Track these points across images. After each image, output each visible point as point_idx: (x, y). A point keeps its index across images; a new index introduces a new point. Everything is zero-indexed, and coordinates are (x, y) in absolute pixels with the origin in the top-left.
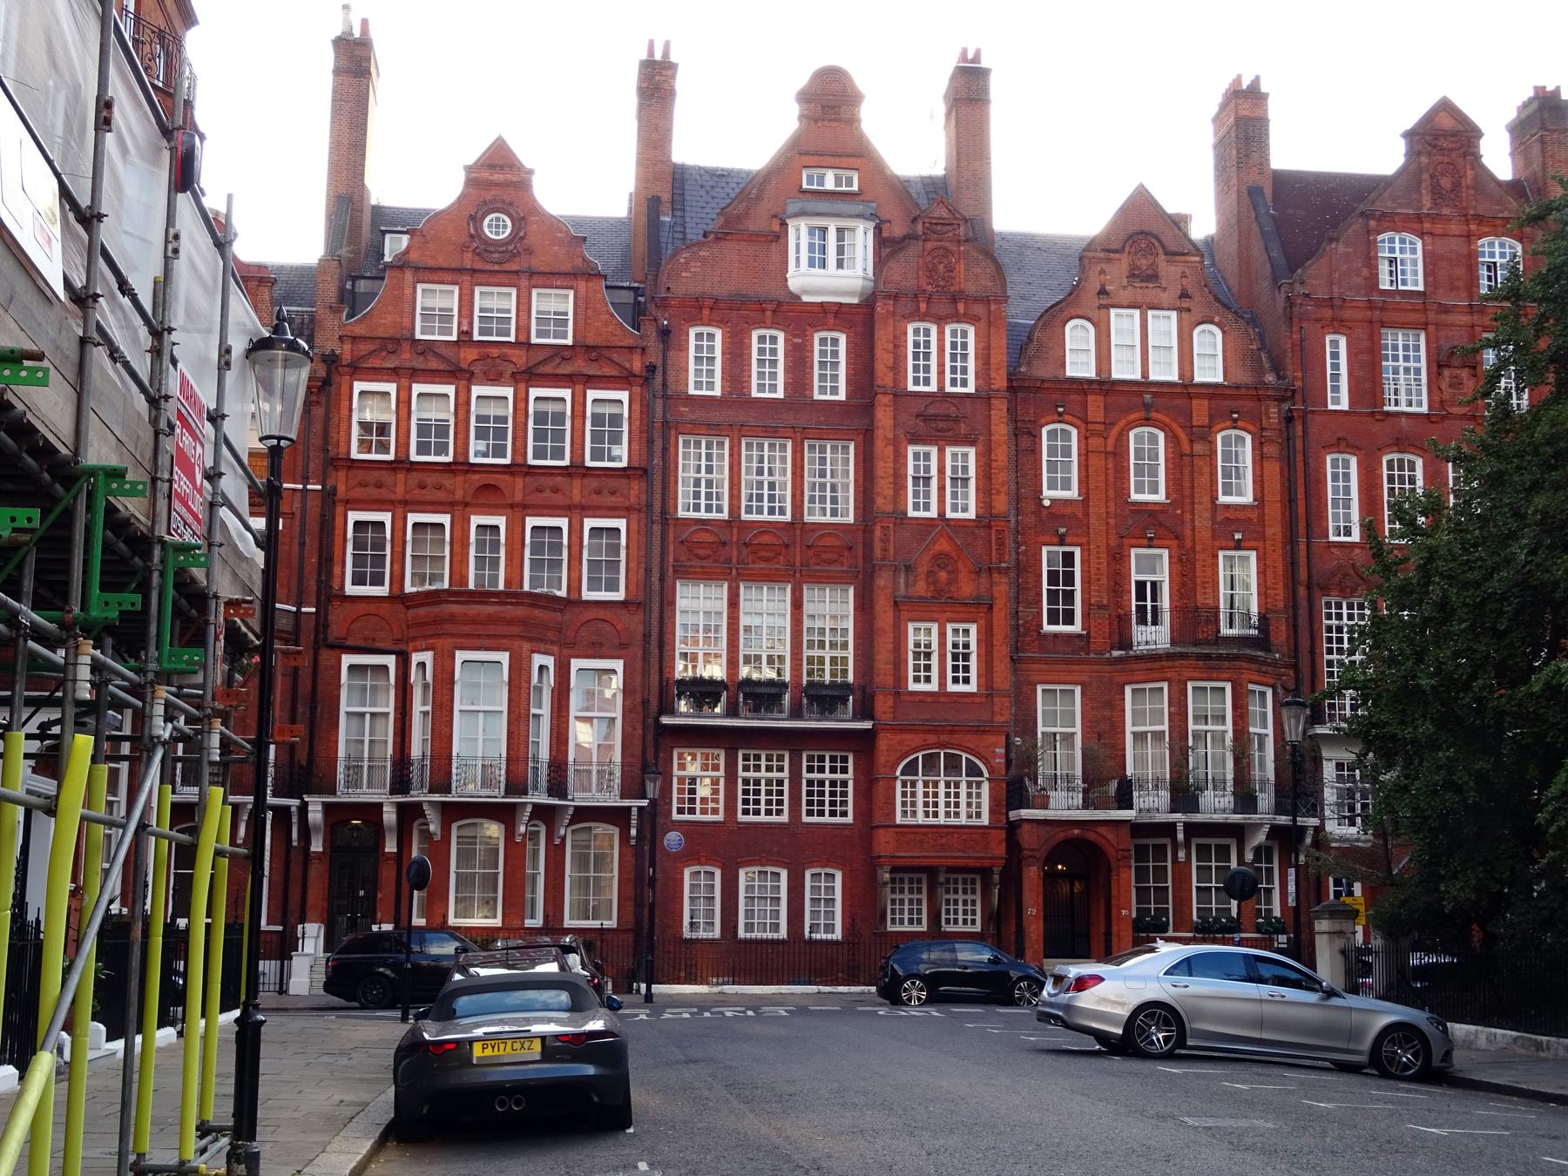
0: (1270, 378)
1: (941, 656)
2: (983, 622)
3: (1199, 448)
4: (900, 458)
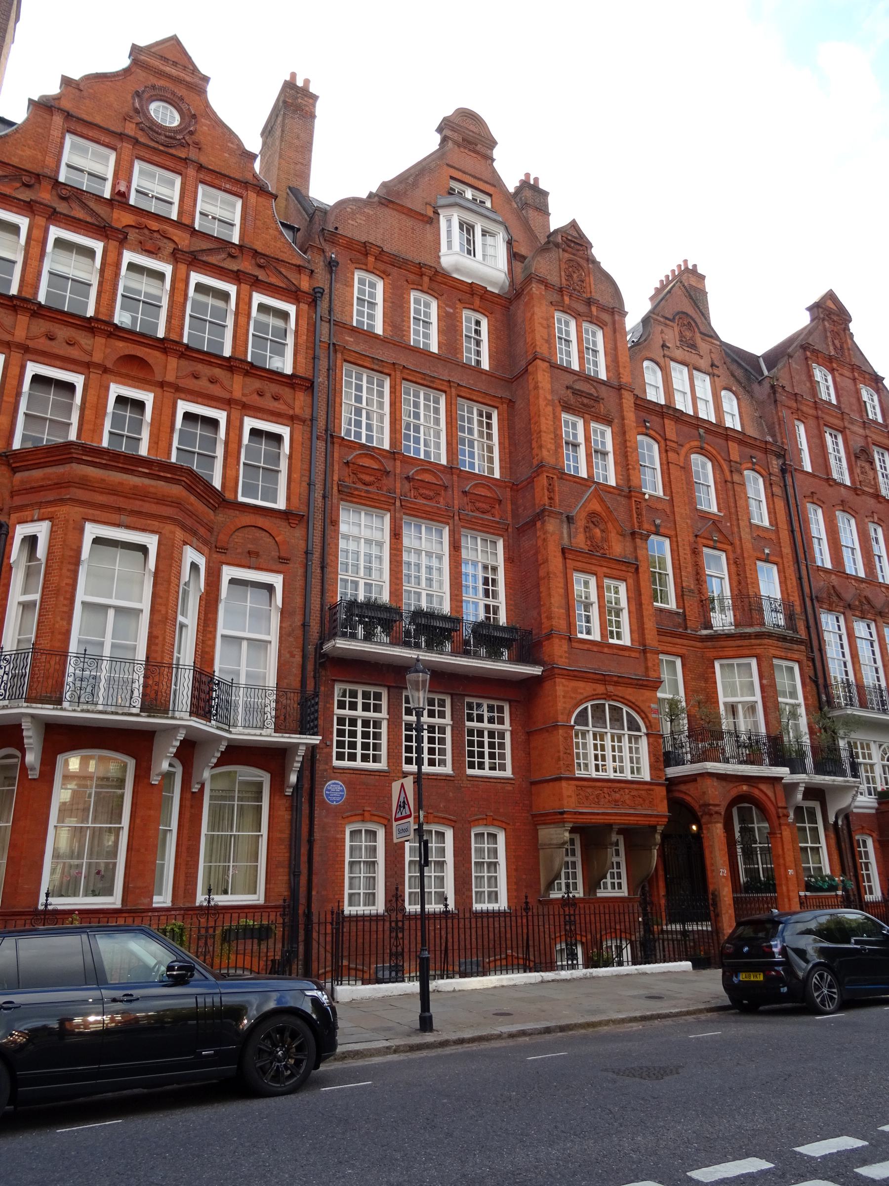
2: (630, 581)
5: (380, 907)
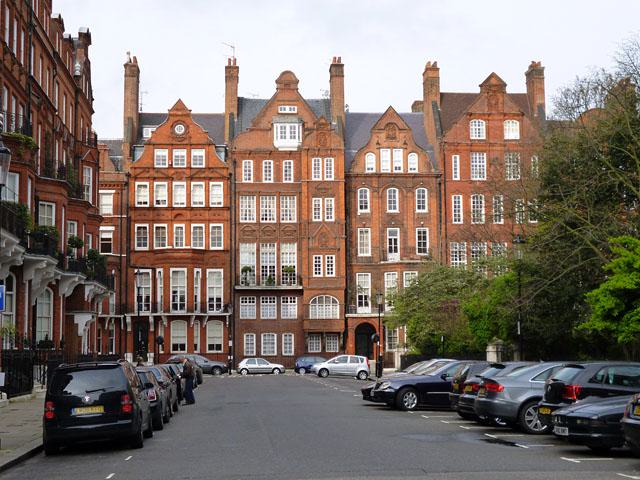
0: (433, 170)
3: (410, 195)
4: (309, 203)
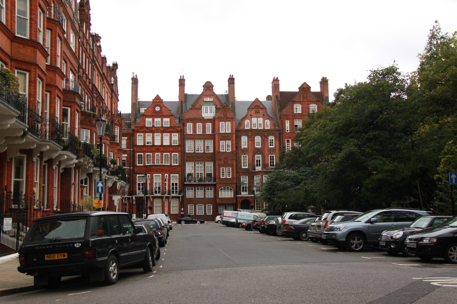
0: (277, 128)
1: (226, 173)
3: (266, 139)
4: (219, 143)
5: (193, 214)
